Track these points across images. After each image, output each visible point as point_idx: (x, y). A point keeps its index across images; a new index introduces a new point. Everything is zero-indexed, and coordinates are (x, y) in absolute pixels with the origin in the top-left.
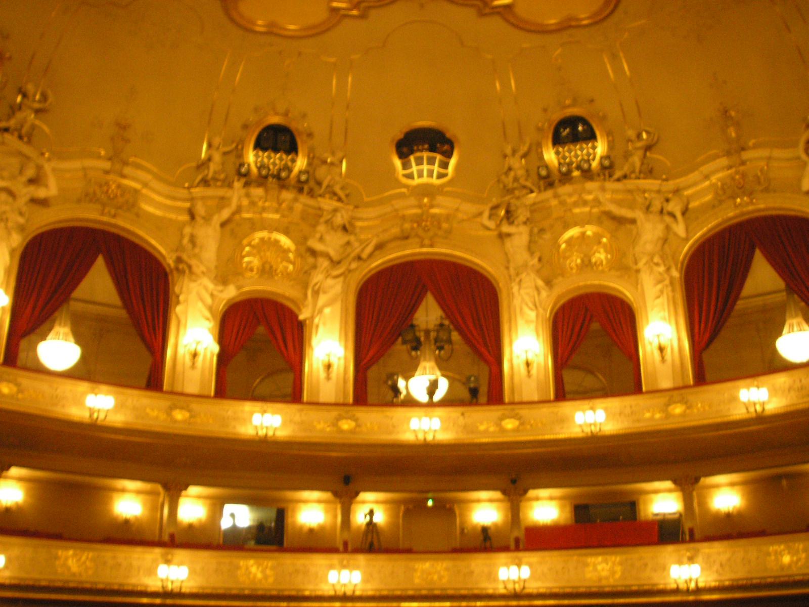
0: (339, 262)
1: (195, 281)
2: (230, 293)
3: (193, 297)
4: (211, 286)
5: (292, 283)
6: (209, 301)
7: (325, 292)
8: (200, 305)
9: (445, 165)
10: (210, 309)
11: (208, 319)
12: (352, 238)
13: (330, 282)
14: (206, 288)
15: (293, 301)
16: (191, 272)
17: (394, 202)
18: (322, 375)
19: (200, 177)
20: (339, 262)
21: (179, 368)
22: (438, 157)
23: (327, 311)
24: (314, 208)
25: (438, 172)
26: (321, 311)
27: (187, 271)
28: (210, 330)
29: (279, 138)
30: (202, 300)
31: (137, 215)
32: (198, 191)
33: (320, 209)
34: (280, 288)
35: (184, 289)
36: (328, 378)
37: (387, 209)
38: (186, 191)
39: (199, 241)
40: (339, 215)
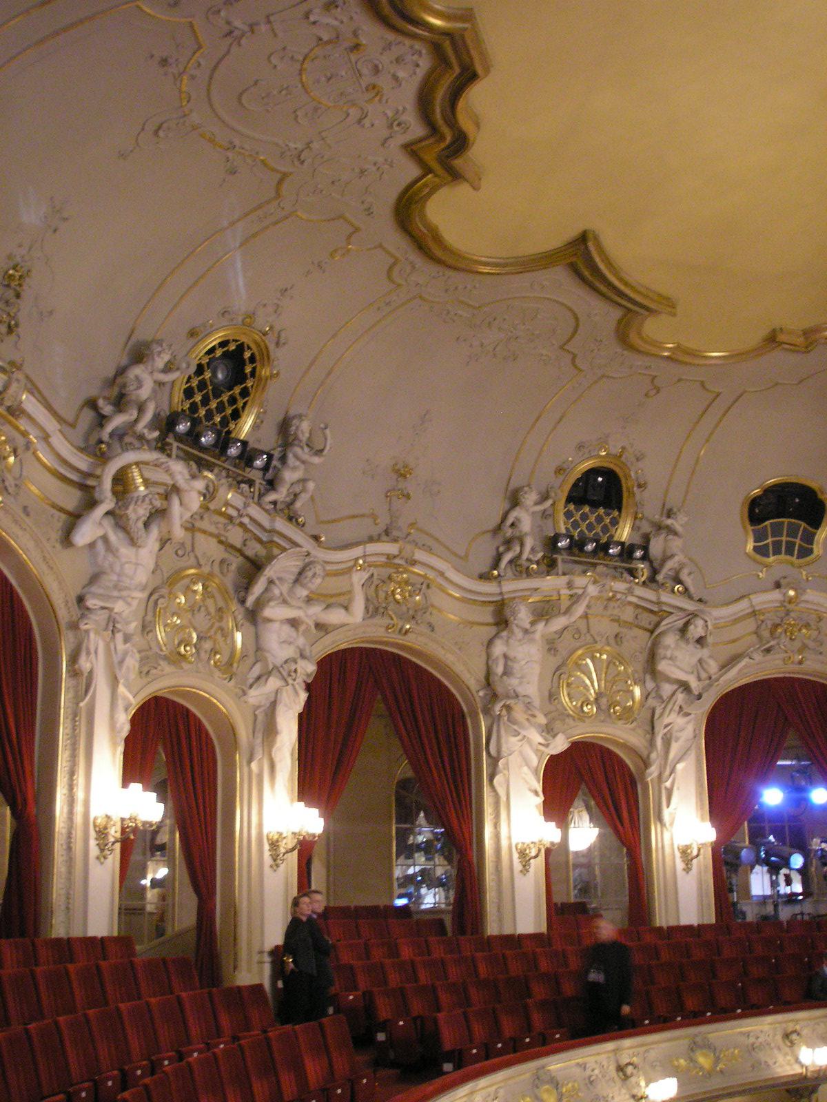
0: (699, 697)
1: (517, 734)
2: (560, 745)
3: (514, 760)
4: (537, 738)
5: (634, 724)
6: (534, 760)
7: (677, 739)
8: (525, 769)
9: (809, 538)
10: (536, 772)
11: (536, 793)
12: (704, 653)
13: (680, 721)
14: (529, 742)
15: (632, 751)
16: (512, 721)
17: (751, 597)
18: (680, 865)
19: (507, 557)
20: (699, 697)
21: (505, 873)
22: (803, 525)
23: (680, 767)
24: (651, 602)
25: (800, 546)
26: (673, 771)
27: (506, 718)
28: (537, 806)
29: (601, 490)
30: (527, 765)
31: (432, 627)
32: (511, 586)
33: (659, 603)
34: (620, 735)
35: (504, 749)
36: (688, 869)
37: (743, 606)
38: (494, 584)
39: (516, 666)
40: (700, 623)
